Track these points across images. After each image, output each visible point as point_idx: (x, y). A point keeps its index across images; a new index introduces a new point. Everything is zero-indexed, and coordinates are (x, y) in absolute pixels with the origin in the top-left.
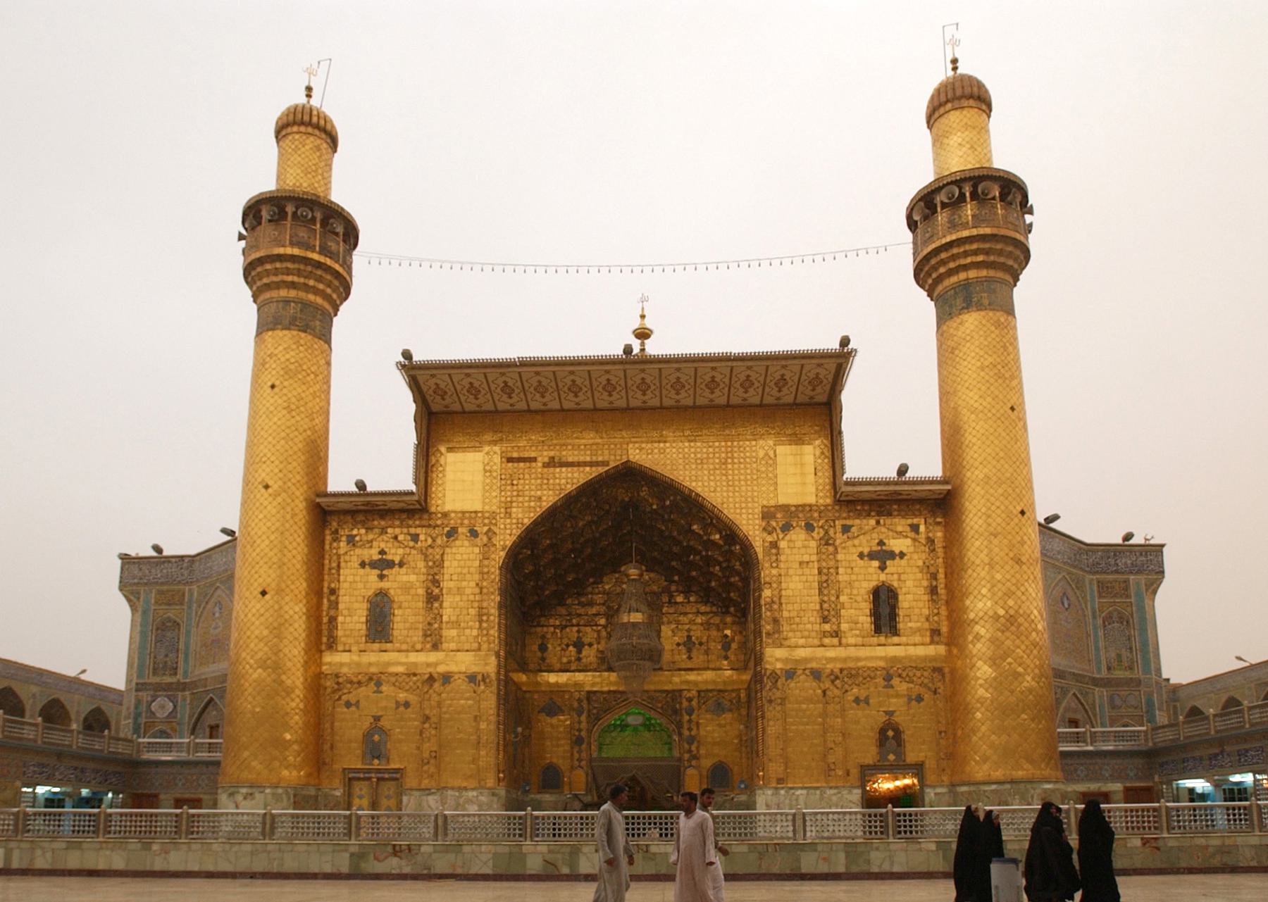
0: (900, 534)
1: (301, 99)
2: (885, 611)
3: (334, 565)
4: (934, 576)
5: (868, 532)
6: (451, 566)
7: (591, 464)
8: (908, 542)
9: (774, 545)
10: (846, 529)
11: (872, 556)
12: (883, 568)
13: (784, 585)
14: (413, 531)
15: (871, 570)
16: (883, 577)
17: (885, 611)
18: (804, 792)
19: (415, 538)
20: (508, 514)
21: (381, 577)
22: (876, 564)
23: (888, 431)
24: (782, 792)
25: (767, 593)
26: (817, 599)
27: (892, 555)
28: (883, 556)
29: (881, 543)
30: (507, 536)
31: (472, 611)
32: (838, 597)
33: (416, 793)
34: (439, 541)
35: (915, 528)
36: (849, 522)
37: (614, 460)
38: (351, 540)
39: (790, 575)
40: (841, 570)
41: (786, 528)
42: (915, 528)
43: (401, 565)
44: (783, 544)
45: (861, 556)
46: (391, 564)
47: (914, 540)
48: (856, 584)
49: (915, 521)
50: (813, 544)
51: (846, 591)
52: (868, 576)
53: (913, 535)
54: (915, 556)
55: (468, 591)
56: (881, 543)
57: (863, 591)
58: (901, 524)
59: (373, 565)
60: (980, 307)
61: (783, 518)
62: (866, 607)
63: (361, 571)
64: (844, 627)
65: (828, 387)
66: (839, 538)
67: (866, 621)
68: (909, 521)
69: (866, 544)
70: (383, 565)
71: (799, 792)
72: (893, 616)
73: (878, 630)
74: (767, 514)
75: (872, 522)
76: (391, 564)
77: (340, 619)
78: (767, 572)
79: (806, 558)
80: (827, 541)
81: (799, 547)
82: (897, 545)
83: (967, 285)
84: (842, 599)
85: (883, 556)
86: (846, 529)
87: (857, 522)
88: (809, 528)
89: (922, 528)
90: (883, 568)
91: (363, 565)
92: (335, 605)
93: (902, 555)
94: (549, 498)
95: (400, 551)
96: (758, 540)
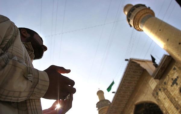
0: (174, 73)
1: (98, 90)
8: (176, 73)
9: (158, 100)
12: (177, 84)
15: (176, 87)
22: (175, 85)
27: (176, 80)
32: (175, 100)
36: (164, 81)
37: (134, 107)
40: (171, 93)
41: (157, 94)
42: (175, 69)
45: (172, 86)
47: (177, 71)
48: (176, 94)
49: (173, 67)
50: (163, 93)
51: (176, 97)
53: (175, 71)
56: (172, 79)
57: (178, 94)
58: (172, 72)
66: (166, 86)
68: (172, 69)
69: (170, 83)
74: (153, 95)
75: (167, 77)
78: (161, 106)
79: (164, 97)
80: (164, 89)
82: (175, 77)
84: (177, 100)
86: (165, 83)
88: (160, 90)
89: (176, 67)
90: (177, 84)
93: (178, 77)
96: (154, 101)
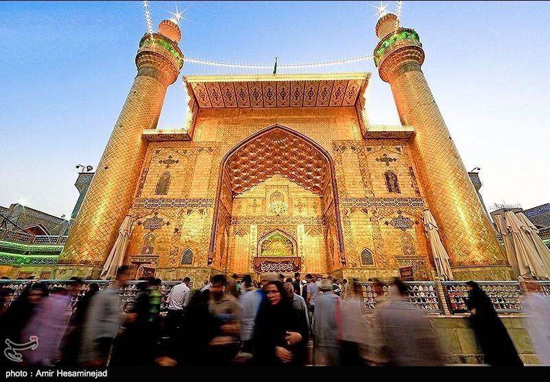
2: (392, 182)
3: (148, 162)
4: (411, 168)
5: (379, 150)
6: (199, 162)
7: (261, 126)
10: (369, 149)
11: (382, 160)
13: (345, 171)
14: (185, 149)
16: (388, 169)
17: (392, 182)
18: (368, 271)
19: (185, 152)
20: (226, 143)
21: (168, 167)
23: (381, 112)
24: (356, 271)
25: (338, 174)
26: (360, 177)
28: (387, 160)
29: (385, 155)
30: (225, 151)
31: (206, 181)
33: (164, 271)
34: (195, 153)
35: (399, 149)
36: (370, 147)
38: (158, 152)
39: (347, 169)
41: (344, 148)
42: (399, 149)
43: (177, 162)
44: (343, 155)
46: (173, 162)
52: (383, 168)
54: (401, 160)
55: (205, 173)
56: (385, 155)
58: (392, 148)
59: (165, 162)
60: (411, 70)
61: (341, 147)
62: (384, 180)
63: (159, 165)
64: (374, 189)
65: (356, 97)
67: (385, 186)
70: (170, 162)
71: (365, 271)
72: (396, 185)
73: (390, 190)
76: (173, 162)
77: (145, 184)
81: (350, 157)
82: (392, 156)
83: (405, 65)
85: (387, 160)
87: (373, 147)
88: (353, 148)
89: (401, 150)
91: (161, 162)
92: (144, 179)
93: (395, 160)
94: (244, 138)
95: (178, 157)
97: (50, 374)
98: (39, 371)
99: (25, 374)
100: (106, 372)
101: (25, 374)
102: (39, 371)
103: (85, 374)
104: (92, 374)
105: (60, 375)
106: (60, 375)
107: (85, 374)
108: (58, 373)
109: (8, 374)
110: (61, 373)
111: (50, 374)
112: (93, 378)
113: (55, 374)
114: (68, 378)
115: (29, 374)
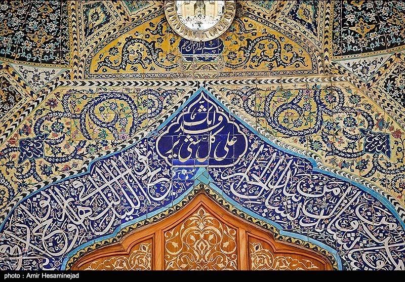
97: (37, 276)
98: (28, 274)
99: (18, 276)
100: (78, 275)
101: (18, 276)
102: (28, 274)
103: (63, 276)
104: (68, 276)
105: (44, 277)
106: (44, 277)
107: (63, 276)
108: (43, 275)
109: (6, 276)
110: (45, 275)
111: (37, 276)
112: (68, 279)
113: (41, 276)
114: (50, 279)
115: (21, 276)
